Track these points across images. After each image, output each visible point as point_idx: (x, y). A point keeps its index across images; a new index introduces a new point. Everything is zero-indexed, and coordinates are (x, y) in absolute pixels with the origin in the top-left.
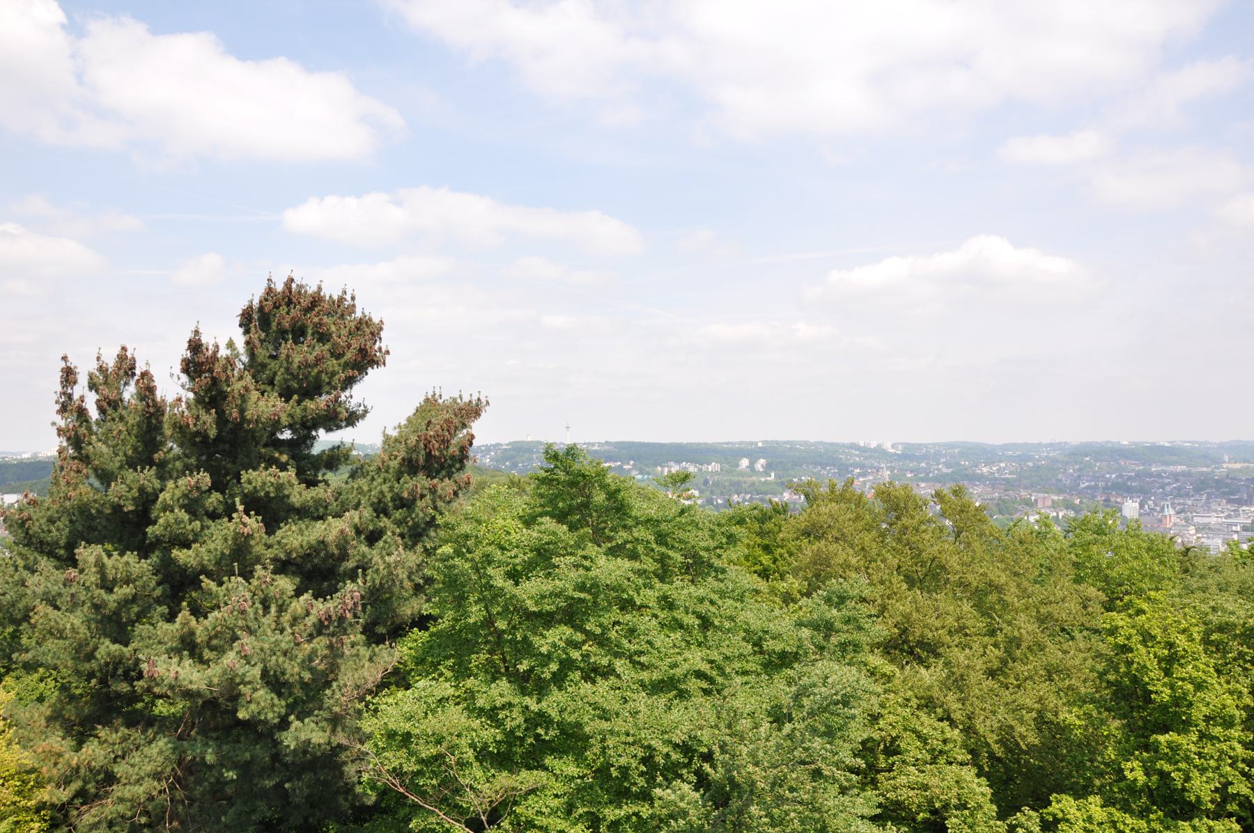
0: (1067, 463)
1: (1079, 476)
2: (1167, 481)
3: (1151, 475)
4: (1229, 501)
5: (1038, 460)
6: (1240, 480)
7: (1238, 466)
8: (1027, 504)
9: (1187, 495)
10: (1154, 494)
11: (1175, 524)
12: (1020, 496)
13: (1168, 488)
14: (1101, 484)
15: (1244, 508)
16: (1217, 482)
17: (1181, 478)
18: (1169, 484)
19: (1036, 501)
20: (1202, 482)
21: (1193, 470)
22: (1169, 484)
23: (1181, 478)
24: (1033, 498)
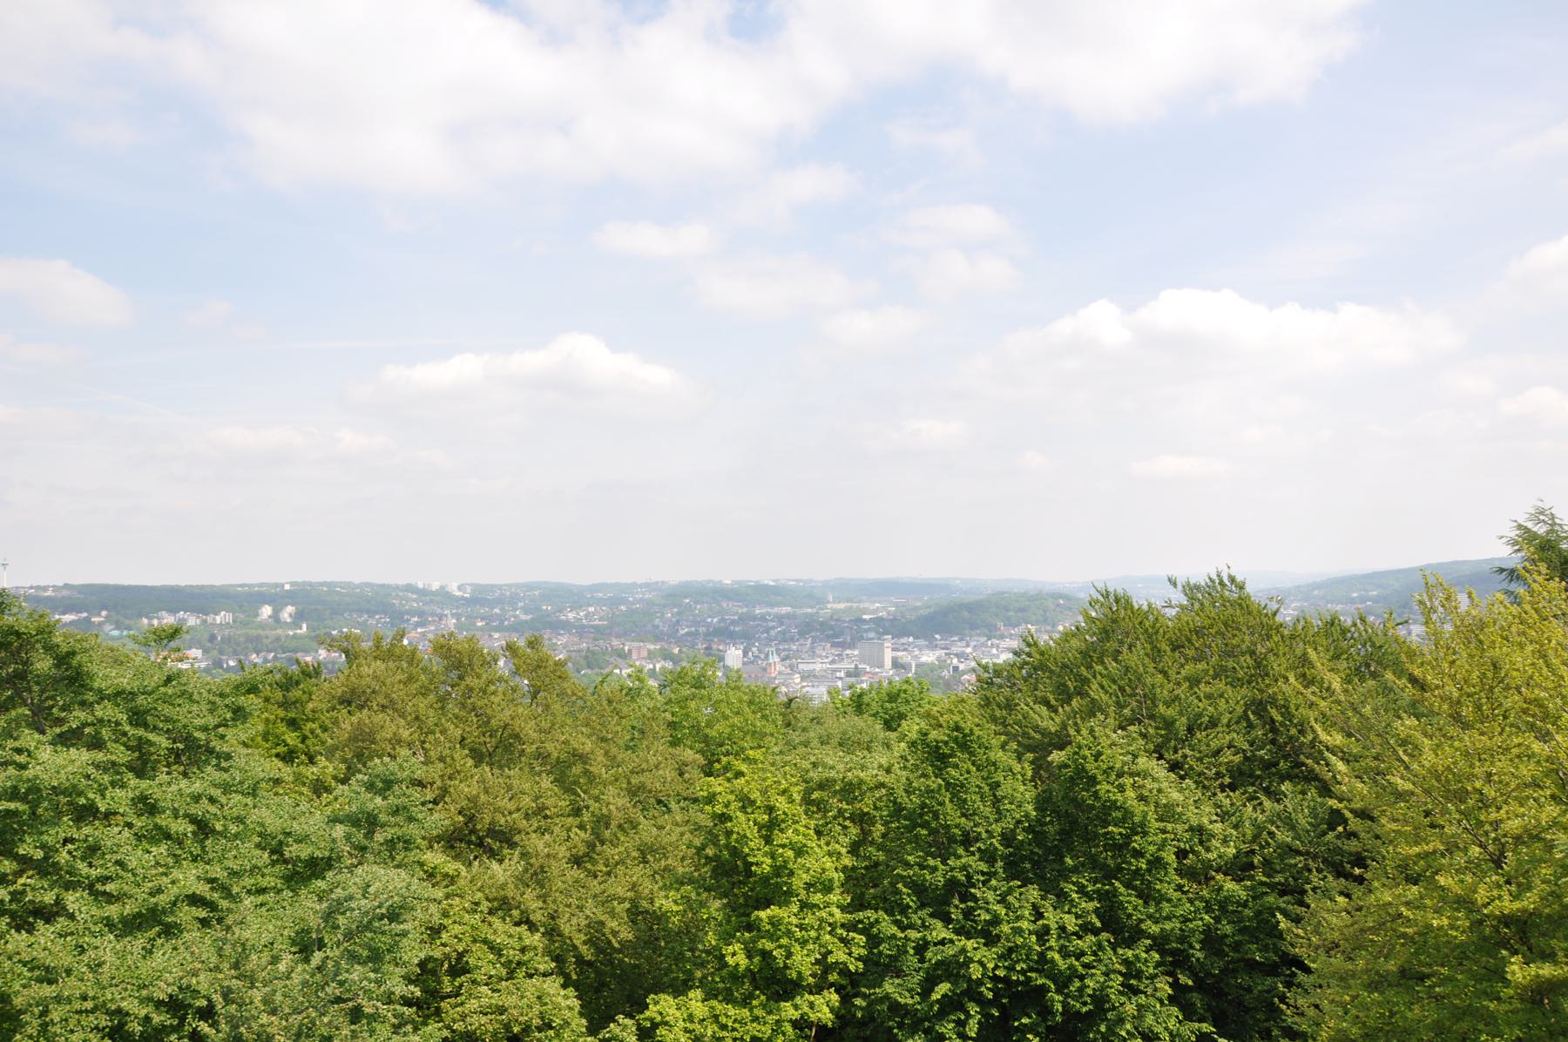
0: (665, 606)
1: (678, 621)
3: (754, 618)
4: (834, 645)
5: (632, 603)
6: (844, 621)
7: (842, 606)
8: (620, 656)
9: (792, 640)
10: (758, 639)
11: (780, 673)
12: (612, 646)
13: (773, 633)
14: (702, 630)
15: (848, 652)
16: (822, 624)
17: (786, 621)
18: (773, 628)
19: (630, 651)
20: (807, 625)
21: (798, 611)
22: (773, 628)
23: (786, 621)
24: (626, 648)
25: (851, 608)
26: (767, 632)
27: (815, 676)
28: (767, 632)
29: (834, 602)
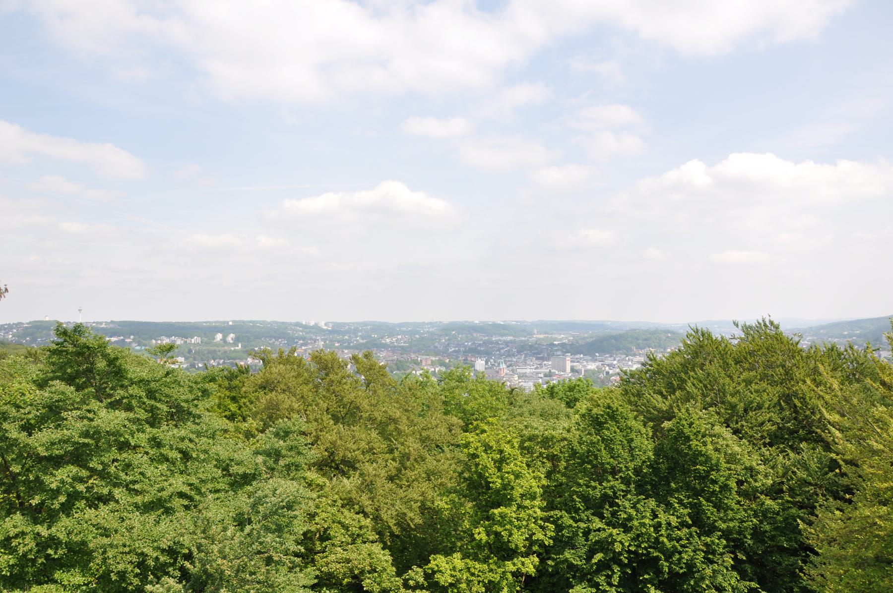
1: (448, 344)
2: (501, 346)
3: (492, 343)
4: (537, 359)
6: (543, 345)
7: (542, 336)
9: (513, 355)
10: (494, 355)
11: (506, 374)
12: (411, 358)
13: (502, 351)
14: (462, 349)
15: (545, 362)
16: (531, 346)
17: (510, 344)
18: (503, 348)
19: (421, 361)
20: (522, 347)
21: (517, 339)
22: (503, 348)
23: (510, 344)
24: (419, 359)
25: (547, 337)
26: (499, 350)
27: (526, 376)
28: (499, 350)
29: (537, 334)
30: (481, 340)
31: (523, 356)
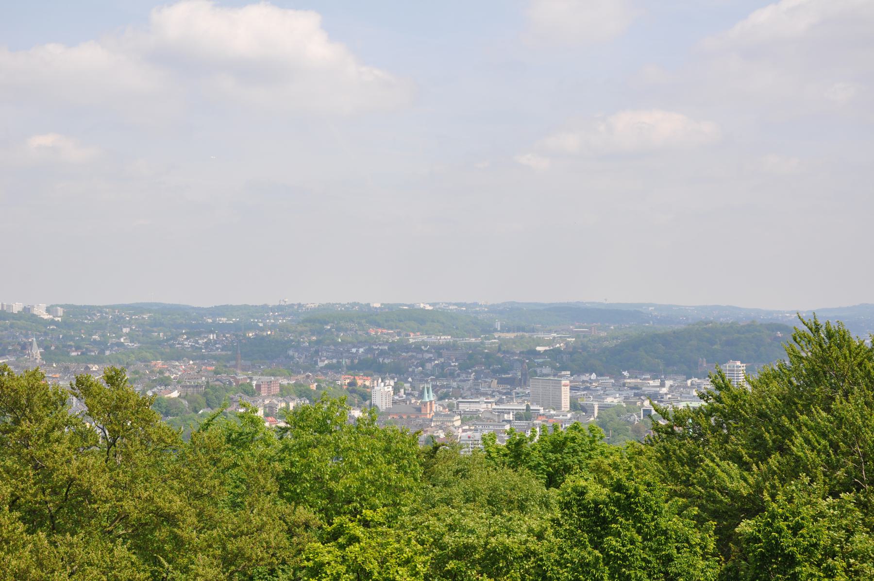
0: (301, 333)
1: (317, 352)
2: (427, 356)
3: (407, 348)
4: (501, 381)
5: (262, 329)
6: (514, 354)
7: (511, 335)
8: (246, 392)
9: (452, 375)
10: (412, 374)
11: (437, 414)
12: (237, 381)
13: (429, 366)
14: (345, 362)
15: (518, 390)
16: (487, 356)
17: (444, 352)
18: (430, 360)
19: (258, 387)
20: (470, 357)
21: (460, 341)
22: (430, 360)
23: (444, 352)
24: (254, 383)
25: (522, 337)
26: (423, 366)
27: (478, 418)
28: (423, 366)
29: (502, 331)
30: (384, 344)
31: (473, 376)
